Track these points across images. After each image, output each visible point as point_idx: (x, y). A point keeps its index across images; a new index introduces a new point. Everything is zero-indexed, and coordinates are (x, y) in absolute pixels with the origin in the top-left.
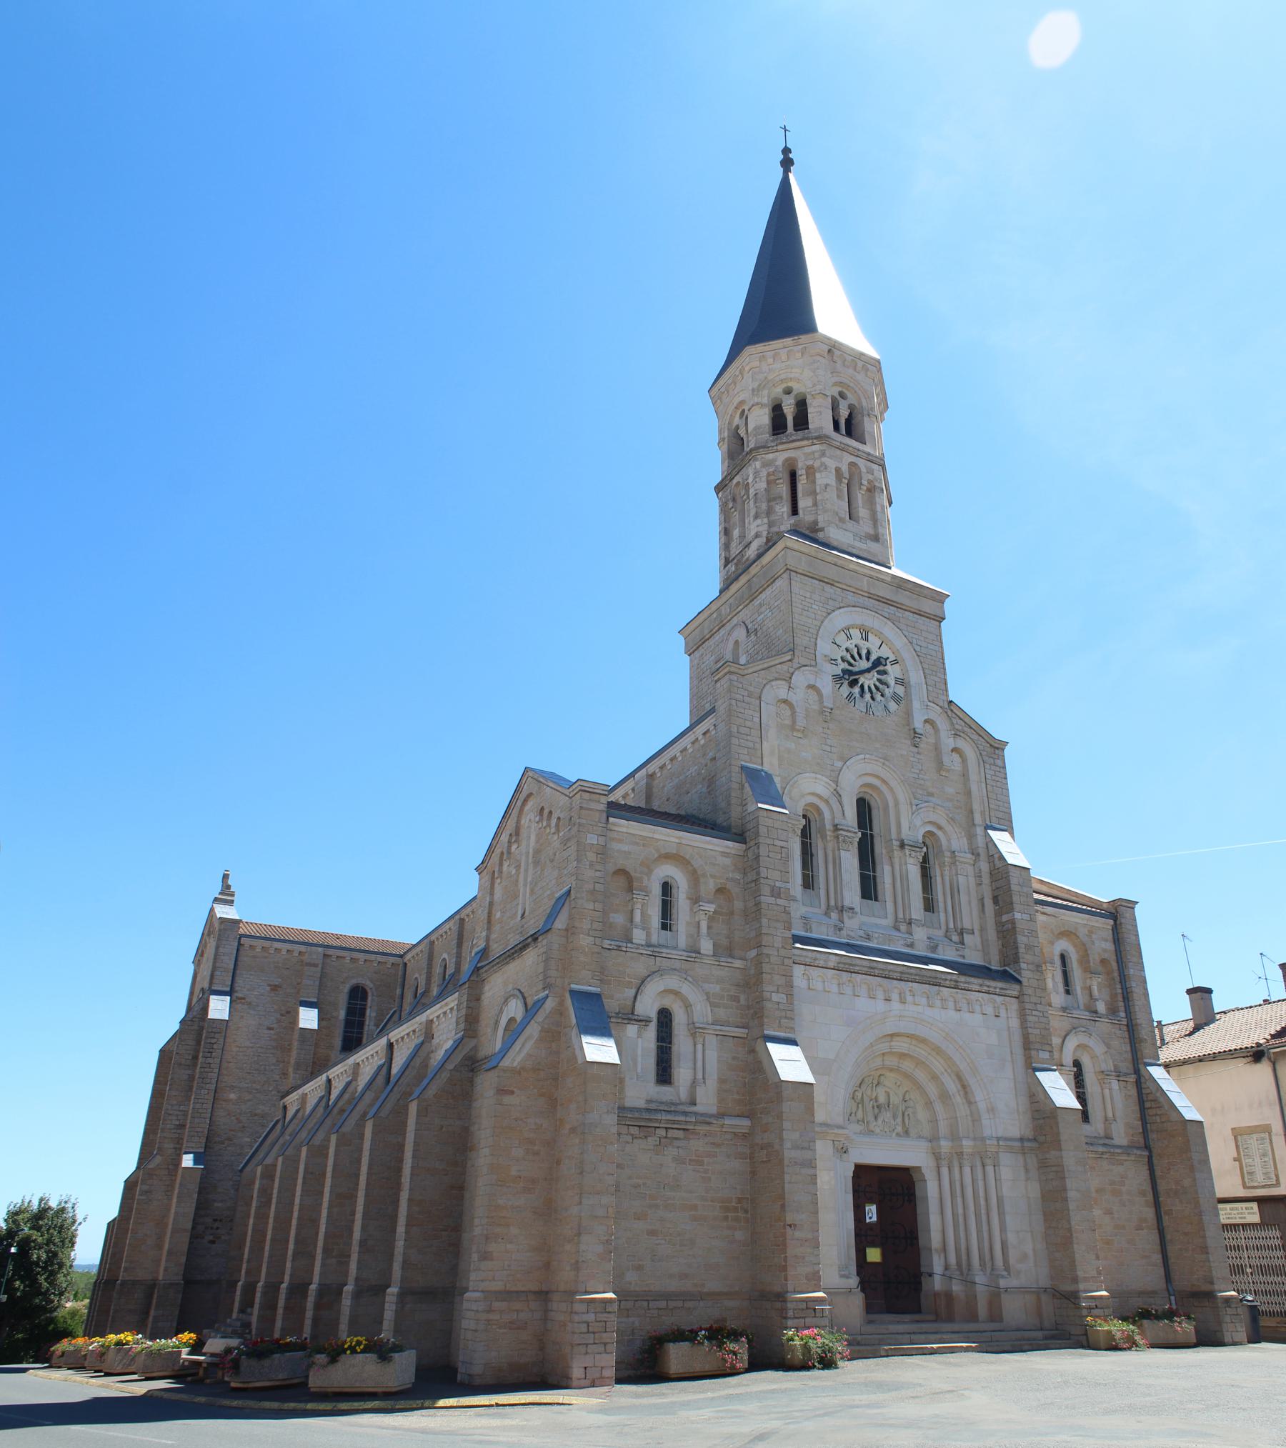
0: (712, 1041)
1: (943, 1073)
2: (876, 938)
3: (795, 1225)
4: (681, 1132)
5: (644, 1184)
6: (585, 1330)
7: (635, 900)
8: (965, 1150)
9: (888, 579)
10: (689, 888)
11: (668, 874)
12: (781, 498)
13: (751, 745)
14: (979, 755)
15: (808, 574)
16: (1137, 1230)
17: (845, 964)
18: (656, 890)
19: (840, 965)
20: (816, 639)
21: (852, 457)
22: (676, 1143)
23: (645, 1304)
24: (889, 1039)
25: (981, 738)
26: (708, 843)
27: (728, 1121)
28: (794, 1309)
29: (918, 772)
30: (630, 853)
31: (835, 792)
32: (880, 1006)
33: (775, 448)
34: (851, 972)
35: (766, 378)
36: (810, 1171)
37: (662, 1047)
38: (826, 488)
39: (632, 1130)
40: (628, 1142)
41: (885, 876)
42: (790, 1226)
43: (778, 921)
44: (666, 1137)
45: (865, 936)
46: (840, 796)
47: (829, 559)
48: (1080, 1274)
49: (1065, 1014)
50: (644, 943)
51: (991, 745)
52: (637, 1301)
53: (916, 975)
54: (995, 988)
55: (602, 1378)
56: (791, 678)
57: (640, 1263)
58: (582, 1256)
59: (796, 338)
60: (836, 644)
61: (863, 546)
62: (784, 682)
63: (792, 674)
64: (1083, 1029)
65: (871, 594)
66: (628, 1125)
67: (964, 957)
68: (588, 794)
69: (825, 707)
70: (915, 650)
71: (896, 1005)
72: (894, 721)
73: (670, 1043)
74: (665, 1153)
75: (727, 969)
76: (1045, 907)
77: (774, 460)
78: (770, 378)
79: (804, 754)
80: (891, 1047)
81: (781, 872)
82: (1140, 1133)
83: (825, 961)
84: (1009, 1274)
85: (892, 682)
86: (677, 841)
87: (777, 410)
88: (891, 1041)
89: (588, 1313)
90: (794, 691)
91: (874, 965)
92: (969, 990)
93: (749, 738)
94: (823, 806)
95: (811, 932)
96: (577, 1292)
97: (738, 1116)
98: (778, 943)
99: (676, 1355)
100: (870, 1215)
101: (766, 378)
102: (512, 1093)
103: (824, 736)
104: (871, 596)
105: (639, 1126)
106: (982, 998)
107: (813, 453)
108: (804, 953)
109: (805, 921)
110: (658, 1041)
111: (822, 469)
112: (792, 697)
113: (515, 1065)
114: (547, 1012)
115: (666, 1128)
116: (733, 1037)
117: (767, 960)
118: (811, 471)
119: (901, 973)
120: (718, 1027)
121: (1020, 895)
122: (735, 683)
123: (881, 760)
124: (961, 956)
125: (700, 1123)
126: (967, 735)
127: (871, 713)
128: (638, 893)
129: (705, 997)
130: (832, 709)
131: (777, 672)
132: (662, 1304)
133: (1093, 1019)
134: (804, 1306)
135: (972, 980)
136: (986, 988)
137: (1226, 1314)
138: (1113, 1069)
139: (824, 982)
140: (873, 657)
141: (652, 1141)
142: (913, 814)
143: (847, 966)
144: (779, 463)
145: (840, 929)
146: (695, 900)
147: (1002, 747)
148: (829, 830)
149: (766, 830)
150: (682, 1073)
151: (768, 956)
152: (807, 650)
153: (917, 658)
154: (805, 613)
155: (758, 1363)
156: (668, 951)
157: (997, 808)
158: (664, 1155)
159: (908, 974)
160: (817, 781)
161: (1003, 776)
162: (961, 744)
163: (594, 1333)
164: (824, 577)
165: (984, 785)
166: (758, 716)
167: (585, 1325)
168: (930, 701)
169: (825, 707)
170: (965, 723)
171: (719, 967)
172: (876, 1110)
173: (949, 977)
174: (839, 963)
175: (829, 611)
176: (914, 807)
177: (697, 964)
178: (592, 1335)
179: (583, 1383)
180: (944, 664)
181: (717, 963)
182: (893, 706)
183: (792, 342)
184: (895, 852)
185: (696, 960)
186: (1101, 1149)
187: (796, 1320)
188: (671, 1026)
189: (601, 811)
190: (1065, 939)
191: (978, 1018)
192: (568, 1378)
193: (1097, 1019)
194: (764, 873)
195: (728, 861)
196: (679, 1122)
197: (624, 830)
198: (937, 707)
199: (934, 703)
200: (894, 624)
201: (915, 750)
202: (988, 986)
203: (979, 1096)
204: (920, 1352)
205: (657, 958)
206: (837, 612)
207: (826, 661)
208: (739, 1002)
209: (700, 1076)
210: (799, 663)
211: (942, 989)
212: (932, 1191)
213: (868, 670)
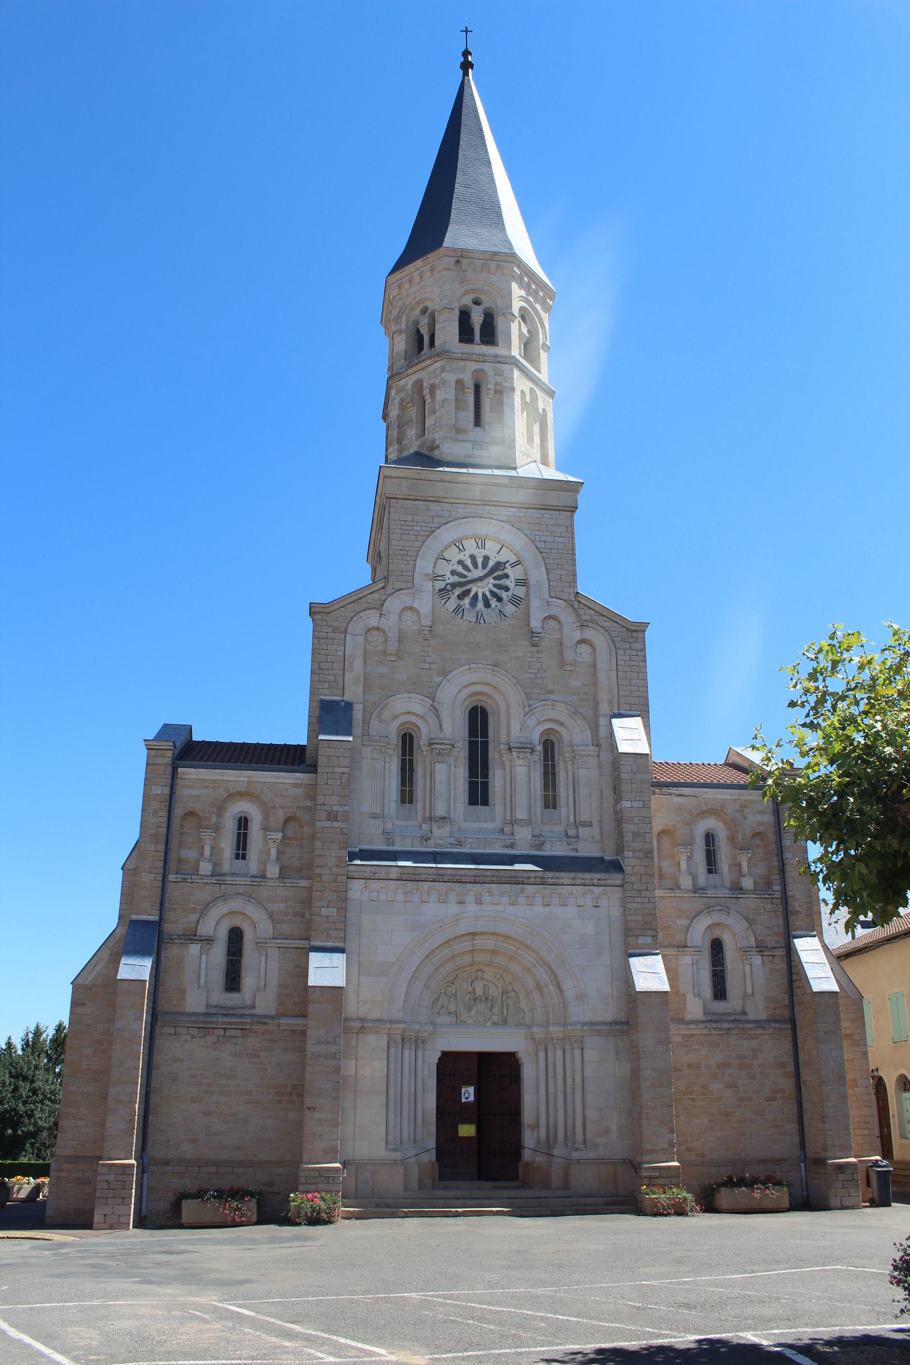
0: (274, 953)
1: (534, 965)
2: (469, 843)
3: (314, 1108)
4: (239, 1031)
5: (201, 1074)
6: (107, 1187)
7: (202, 837)
8: (554, 1035)
9: (506, 481)
10: (263, 819)
11: (241, 810)
12: (412, 420)
13: (332, 678)
14: (610, 641)
15: (409, 497)
16: (767, 1101)
17: (409, 874)
18: (230, 825)
19: (402, 876)
20: (415, 560)
21: (478, 363)
22: (235, 1040)
23: (197, 1169)
24: (471, 937)
25: (614, 624)
26: (278, 777)
27: (283, 1021)
28: (306, 1177)
29: (536, 671)
30: (199, 796)
31: (432, 708)
32: (452, 909)
33: (406, 373)
34: (418, 881)
35: (404, 304)
36: (334, 1063)
37: (231, 960)
38: (443, 404)
39: (191, 1030)
40: (187, 1041)
41: (497, 780)
42: (309, 1109)
43: (333, 842)
44: (224, 1036)
45: (456, 843)
46: (437, 710)
47: (435, 477)
48: (647, 1146)
49: (697, 895)
50: (209, 873)
51: (628, 629)
52: (189, 1166)
53: (493, 876)
54: (592, 879)
55: (119, 1223)
56: (382, 605)
57: (196, 1137)
58: (108, 1131)
59: (425, 258)
60: (445, 559)
62: (374, 611)
63: (384, 601)
64: (720, 908)
65: (485, 501)
66: (188, 1027)
67: (577, 850)
68: (155, 751)
69: (422, 626)
70: (537, 548)
71: (471, 908)
72: (510, 625)
73: (240, 956)
74: (223, 1049)
75: (292, 889)
76: (679, 789)
77: (406, 385)
78: (408, 303)
79: (398, 676)
80: (473, 945)
81: (340, 796)
82: (786, 1006)
83: (386, 873)
84: (586, 1148)
85: (512, 586)
86: (246, 779)
87: (464, 317)
88: (473, 940)
89: (109, 1174)
90: (387, 617)
91: (443, 871)
92: (560, 885)
93: (330, 672)
94: (420, 723)
95: (393, 845)
96: (101, 1158)
97: (297, 1016)
98: (332, 861)
99: (189, 1208)
100: (467, 1095)
101: (404, 304)
102: (84, 1004)
103: (423, 654)
104: (486, 503)
105: (199, 1028)
106: (577, 890)
107: (435, 370)
108: (363, 868)
109: (388, 836)
110: (228, 956)
111: (441, 385)
112: (384, 624)
113: (87, 982)
114: (117, 938)
115: (224, 1029)
116: (296, 948)
117: (318, 879)
118: (433, 388)
119: (475, 876)
120: (279, 941)
121: (632, 783)
122: (319, 622)
123: (489, 667)
124: (573, 849)
125: (255, 1023)
126: (597, 624)
127: (482, 621)
128: (204, 830)
129: (268, 916)
130: (430, 627)
131: (367, 602)
132: (213, 1169)
133: (736, 896)
134: (317, 1174)
135: (562, 874)
136: (580, 881)
137: (838, 1180)
138: (754, 945)
139: (387, 892)
140: (491, 564)
141: (210, 1039)
142: (525, 715)
143: (411, 876)
144: (409, 387)
145: (427, 840)
146: (266, 829)
147: (642, 628)
148: (424, 746)
149: (325, 759)
150: (248, 981)
151: (320, 875)
152: (404, 573)
153: (539, 554)
154: (403, 537)
155: (263, 1219)
156: (232, 879)
157: (630, 694)
158: (221, 1051)
159: (482, 876)
160: (411, 700)
161: (642, 659)
162: (589, 634)
163: (114, 1189)
164: (428, 496)
165: (614, 673)
166: (343, 649)
167: (106, 1183)
168: (552, 597)
169: (422, 626)
170: (595, 611)
171: (285, 888)
172: (472, 1002)
173: (533, 875)
174: (402, 874)
175: (433, 529)
176: (527, 708)
177: (261, 887)
178: (112, 1191)
179: (102, 1225)
180: (574, 554)
181: (283, 885)
182: (510, 609)
183: (422, 263)
184: (504, 755)
185: (260, 883)
186: (726, 1025)
187: (307, 1186)
188: (242, 942)
189: (166, 765)
190: (712, 817)
191: (572, 911)
192: (92, 1224)
193: (739, 896)
194: (320, 799)
195: (300, 791)
196: (235, 1023)
197: (194, 777)
198: (562, 602)
199: (557, 598)
200: (512, 526)
201: (535, 649)
202: (583, 879)
203: (567, 985)
204: (444, 1214)
205: (222, 885)
206: (443, 528)
207: (426, 580)
208: (304, 916)
209: (262, 983)
210: (394, 589)
211: (525, 886)
212: (528, 1072)
213: (481, 579)
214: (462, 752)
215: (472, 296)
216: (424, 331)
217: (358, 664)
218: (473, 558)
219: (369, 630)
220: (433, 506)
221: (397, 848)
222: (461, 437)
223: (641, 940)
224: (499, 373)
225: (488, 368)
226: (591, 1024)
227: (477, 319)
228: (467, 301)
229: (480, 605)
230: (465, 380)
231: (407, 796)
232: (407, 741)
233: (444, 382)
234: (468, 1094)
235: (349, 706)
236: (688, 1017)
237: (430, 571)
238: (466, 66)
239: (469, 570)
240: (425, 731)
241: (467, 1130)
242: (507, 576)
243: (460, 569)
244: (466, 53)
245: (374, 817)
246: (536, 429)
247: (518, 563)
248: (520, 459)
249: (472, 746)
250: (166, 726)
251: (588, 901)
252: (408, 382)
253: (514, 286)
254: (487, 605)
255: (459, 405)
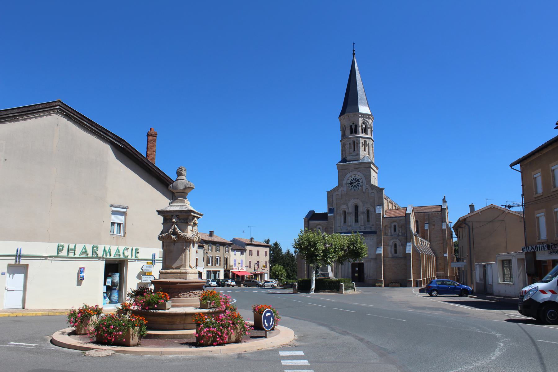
9: (358, 164)
41: (359, 218)
61: (355, 158)
85: (360, 183)
94: (346, 210)
118: (346, 145)
140: (357, 179)
162: (373, 191)
165: (377, 198)
182: (360, 188)
213: (355, 183)
214: (354, 214)
215: (352, 122)
216: (345, 130)
217: (335, 201)
218: (354, 178)
219: (336, 195)
220: (346, 170)
221: (342, 231)
222: (351, 154)
223: (379, 245)
224: (357, 140)
225: (355, 139)
226: (372, 258)
227: (353, 127)
228: (351, 124)
229: (355, 188)
230: (351, 142)
231: (345, 222)
232: (345, 212)
233: (347, 144)
234: (357, 269)
235: (334, 208)
236: (389, 257)
237: (346, 183)
238: (354, 54)
239: (353, 181)
240: (347, 211)
241: (356, 275)
242: (359, 181)
243: (351, 181)
244: (354, 51)
245: (339, 226)
246: (367, 148)
247: (361, 178)
248: (361, 157)
249: (355, 212)
250: (310, 211)
251: (372, 239)
252: (343, 142)
253: (360, 119)
254: (356, 187)
255: (350, 147)
